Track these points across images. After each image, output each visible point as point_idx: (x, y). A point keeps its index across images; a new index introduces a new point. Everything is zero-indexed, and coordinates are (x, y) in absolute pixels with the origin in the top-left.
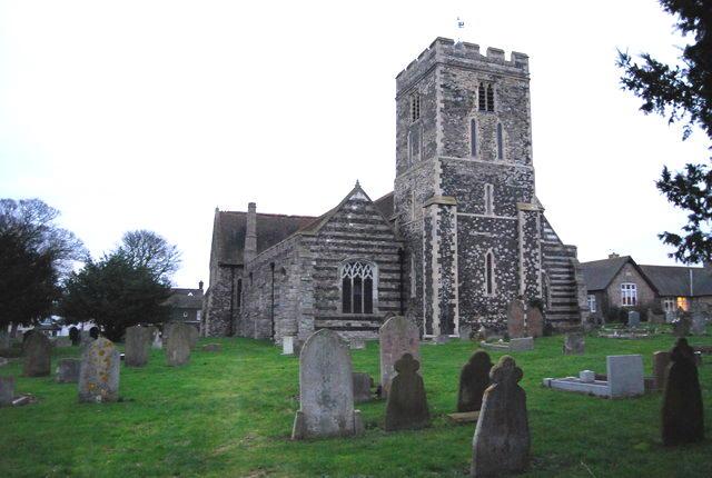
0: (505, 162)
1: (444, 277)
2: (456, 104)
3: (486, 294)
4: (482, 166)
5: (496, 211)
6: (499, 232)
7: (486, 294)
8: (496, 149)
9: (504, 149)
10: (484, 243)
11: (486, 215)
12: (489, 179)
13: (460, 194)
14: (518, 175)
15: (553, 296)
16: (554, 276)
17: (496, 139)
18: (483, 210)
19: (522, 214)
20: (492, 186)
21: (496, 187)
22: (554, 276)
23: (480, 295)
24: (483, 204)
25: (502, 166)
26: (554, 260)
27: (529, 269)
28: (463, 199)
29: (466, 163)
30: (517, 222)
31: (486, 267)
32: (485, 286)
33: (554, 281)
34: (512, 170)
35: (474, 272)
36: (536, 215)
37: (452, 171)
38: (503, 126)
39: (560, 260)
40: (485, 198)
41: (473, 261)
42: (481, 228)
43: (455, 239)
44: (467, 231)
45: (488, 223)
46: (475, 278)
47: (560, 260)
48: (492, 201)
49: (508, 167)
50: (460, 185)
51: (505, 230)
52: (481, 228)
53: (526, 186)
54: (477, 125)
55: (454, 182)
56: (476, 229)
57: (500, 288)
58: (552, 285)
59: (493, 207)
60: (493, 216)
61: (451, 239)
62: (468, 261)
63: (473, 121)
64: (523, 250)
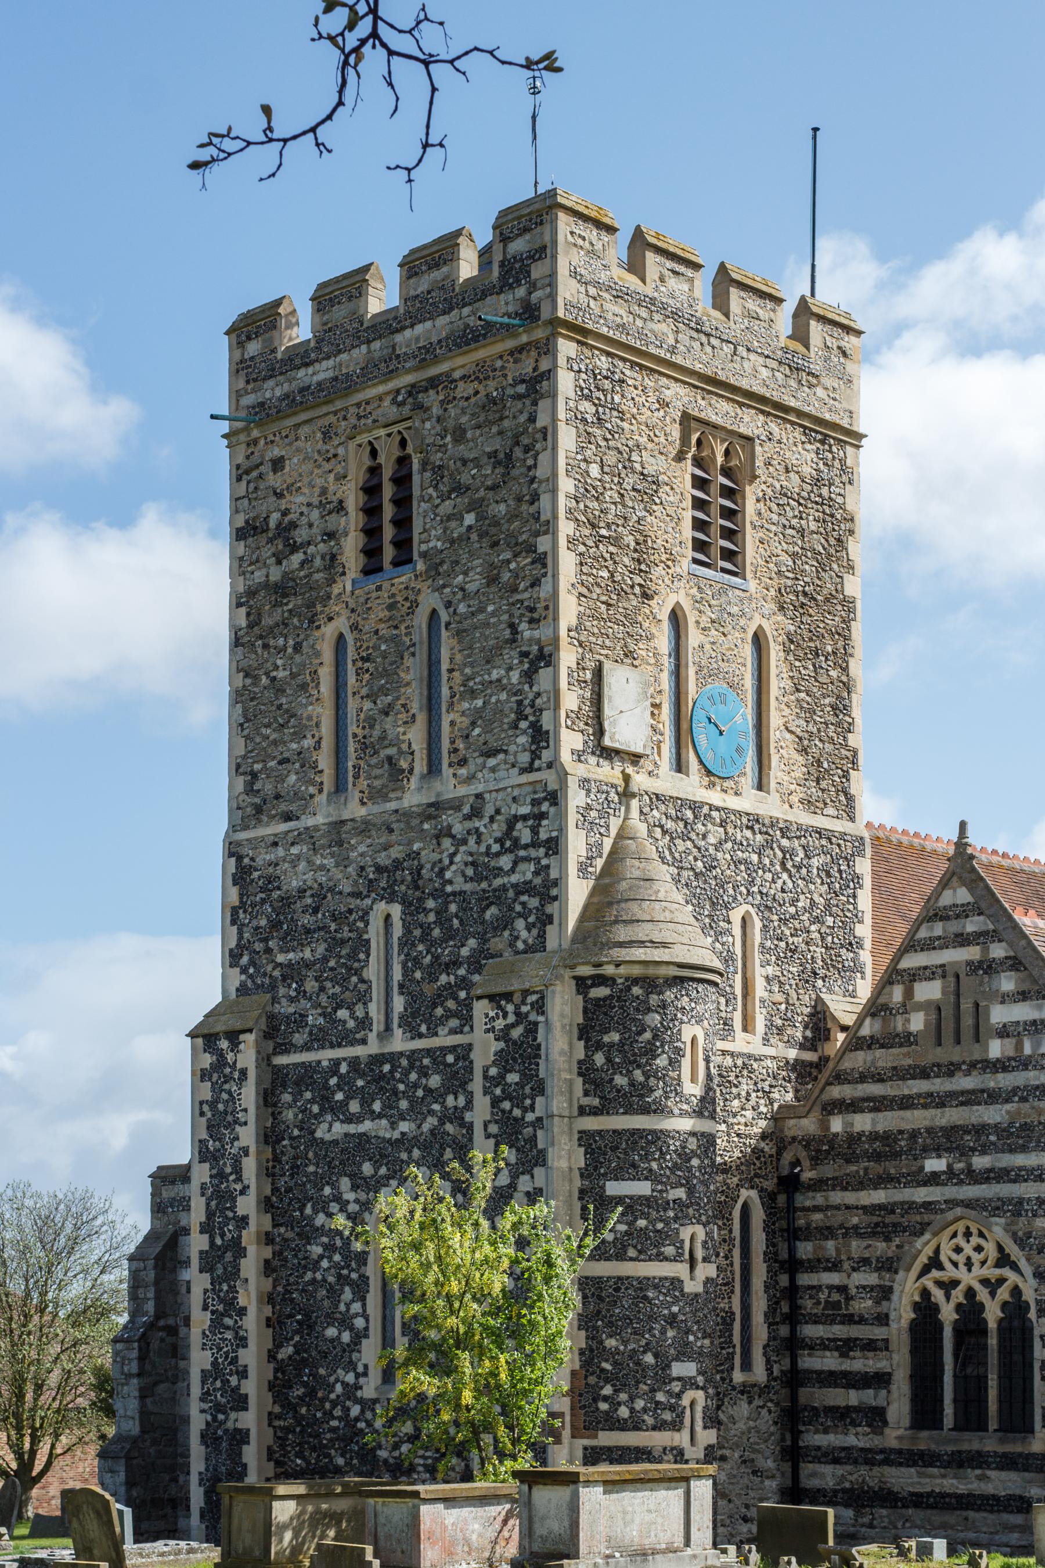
0: (450, 786)
1: (217, 1324)
2: (281, 590)
4: (364, 828)
5: (410, 1025)
6: (417, 1111)
7: (369, 1389)
8: (416, 736)
9: (446, 720)
10: (367, 1168)
11: (373, 1047)
12: (385, 880)
13: (292, 973)
14: (498, 828)
17: (414, 695)
18: (365, 1023)
19: (481, 1009)
20: (396, 910)
21: (412, 908)
23: (351, 1391)
24: (364, 998)
25: (436, 807)
28: (301, 992)
29: (307, 835)
30: (464, 1052)
34: (476, 813)
35: (334, 1294)
36: (540, 1007)
37: (271, 882)
38: (444, 616)
40: (373, 971)
41: (330, 1248)
42: (354, 1107)
43: (250, 1166)
44: (307, 1127)
45: (378, 1078)
46: (331, 1319)
48: (397, 974)
49: (455, 805)
50: (295, 937)
51: (437, 1094)
52: (354, 1107)
53: (526, 872)
54: (351, 653)
55: (275, 925)
56: (339, 1111)
59: (399, 1003)
60: (399, 1043)
61: (238, 1170)
62: (316, 1250)
63: (340, 640)
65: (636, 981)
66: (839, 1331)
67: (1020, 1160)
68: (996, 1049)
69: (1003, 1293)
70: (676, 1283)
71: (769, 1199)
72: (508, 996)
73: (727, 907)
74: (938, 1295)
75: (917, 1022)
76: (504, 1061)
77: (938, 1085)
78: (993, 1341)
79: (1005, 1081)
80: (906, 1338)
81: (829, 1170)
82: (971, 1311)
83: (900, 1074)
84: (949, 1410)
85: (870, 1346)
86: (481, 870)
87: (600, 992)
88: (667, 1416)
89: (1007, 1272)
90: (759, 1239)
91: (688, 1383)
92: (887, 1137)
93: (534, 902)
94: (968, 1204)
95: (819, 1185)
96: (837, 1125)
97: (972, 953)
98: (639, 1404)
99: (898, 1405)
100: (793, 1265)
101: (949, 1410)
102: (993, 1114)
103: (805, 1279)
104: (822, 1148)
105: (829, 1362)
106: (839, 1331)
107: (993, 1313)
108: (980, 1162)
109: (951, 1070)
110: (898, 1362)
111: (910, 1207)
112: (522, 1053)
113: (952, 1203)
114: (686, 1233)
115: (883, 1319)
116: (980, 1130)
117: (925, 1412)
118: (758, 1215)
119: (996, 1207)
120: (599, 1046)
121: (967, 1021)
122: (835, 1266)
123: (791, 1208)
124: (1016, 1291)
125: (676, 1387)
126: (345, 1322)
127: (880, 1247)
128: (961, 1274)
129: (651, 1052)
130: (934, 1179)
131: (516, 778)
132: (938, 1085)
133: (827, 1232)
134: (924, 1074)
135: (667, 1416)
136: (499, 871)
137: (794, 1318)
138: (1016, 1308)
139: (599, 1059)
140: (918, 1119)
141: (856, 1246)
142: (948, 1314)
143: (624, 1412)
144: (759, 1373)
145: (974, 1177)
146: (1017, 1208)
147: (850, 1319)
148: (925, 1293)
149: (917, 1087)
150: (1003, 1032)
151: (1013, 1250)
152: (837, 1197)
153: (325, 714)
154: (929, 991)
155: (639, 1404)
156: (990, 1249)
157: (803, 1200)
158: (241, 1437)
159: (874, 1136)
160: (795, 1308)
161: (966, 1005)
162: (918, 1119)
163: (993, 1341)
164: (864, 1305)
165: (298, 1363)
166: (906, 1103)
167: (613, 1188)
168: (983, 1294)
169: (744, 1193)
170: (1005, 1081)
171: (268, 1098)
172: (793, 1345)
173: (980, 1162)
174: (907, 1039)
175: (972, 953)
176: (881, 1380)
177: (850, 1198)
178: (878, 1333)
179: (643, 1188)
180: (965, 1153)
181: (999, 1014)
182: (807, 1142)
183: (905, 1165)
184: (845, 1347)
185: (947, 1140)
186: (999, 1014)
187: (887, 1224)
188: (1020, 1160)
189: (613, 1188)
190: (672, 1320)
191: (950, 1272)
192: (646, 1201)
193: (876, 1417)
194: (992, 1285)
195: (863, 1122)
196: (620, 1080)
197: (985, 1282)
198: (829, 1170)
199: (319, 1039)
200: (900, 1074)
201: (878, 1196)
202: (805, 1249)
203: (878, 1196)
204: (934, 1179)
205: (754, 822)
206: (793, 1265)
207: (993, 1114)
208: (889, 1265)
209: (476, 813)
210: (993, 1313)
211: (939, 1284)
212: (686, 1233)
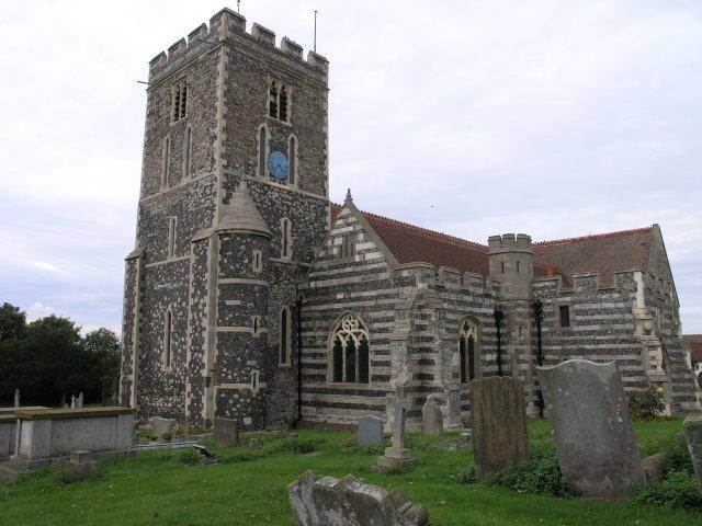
3: (163, 366)
6: (178, 280)
11: (169, 260)
15: (376, 364)
16: (376, 326)
18: (167, 253)
20: (176, 218)
21: (180, 216)
22: (376, 326)
23: (159, 368)
26: (377, 297)
27: (195, 329)
31: (165, 330)
32: (163, 358)
33: (377, 336)
34: (197, 187)
35: (156, 338)
39: (387, 296)
42: (163, 279)
47: (387, 296)
52: (163, 279)
57: (175, 359)
58: (373, 342)
64: (191, 301)
65: (238, 235)
66: (312, 351)
67: (365, 294)
68: (357, 258)
69: (360, 338)
70: (249, 334)
71: (292, 309)
72: (200, 241)
73: (279, 218)
74: (341, 338)
75: (335, 251)
76: (198, 262)
77: (341, 271)
78: (357, 353)
79: (359, 269)
80: (332, 353)
81: (311, 299)
82: (351, 343)
83: (330, 268)
84: (344, 376)
85: (321, 355)
86: (197, 204)
87: (226, 239)
88: (245, 379)
89: (361, 330)
90: (289, 320)
91: (252, 367)
92: (326, 288)
93: (209, 212)
94: (350, 309)
95: (307, 304)
96: (312, 284)
97: (351, 229)
98: (235, 374)
99: (330, 373)
100: (300, 330)
101: (344, 376)
102: (356, 279)
103: (303, 334)
104: (309, 293)
105: (310, 360)
106: (312, 351)
107: (357, 344)
108: (353, 295)
109: (345, 266)
110: (330, 361)
111: (332, 310)
112: (202, 260)
113: (345, 308)
114: (253, 318)
115: (325, 346)
116: (353, 284)
117: (338, 378)
118: (289, 314)
119: (357, 309)
120: (226, 256)
121: (349, 250)
122: (311, 330)
123: (299, 312)
124: (364, 336)
125: (248, 369)
126: (158, 347)
127: (325, 324)
128: (347, 331)
129: (242, 258)
130: (339, 301)
131: (207, 174)
132: (341, 271)
133: (310, 319)
134: (337, 268)
135: (245, 379)
136: (201, 203)
137: (300, 347)
138: (364, 342)
139: (225, 261)
140: (334, 282)
141: (318, 323)
142: (344, 344)
143: (230, 377)
144: (288, 364)
145: (352, 300)
146: (363, 309)
147: (315, 347)
148: (338, 338)
149: (335, 271)
150: (359, 253)
151: (363, 323)
152: (313, 308)
153: (163, 162)
154: (339, 241)
155: (235, 374)
156: (357, 324)
157: (304, 309)
158: (130, 382)
159: (323, 288)
160: (300, 343)
161: (349, 244)
162: (334, 282)
163: (357, 353)
164: (319, 342)
165: (147, 360)
166: (332, 277)
167: (228, 303)
168: (354, 337)
169: (284, 307)
170: (359, 269)
171: (142, 278)
172: (300, 355)
173: (353, 295)
174: (333, 257)
175: (351, 229)
176: (324, 366)
177: (316, 308)
178: (324, 351)
179: (238, 302)
180: (349, 292)
181: (359, 247)
182: (304, 291)
183: (330, 297)
184: (314, 356)
185: (345, 288)
186: (359, 247)
187: (326, 316)
188: (365, 294)
189: (228, 303)
190: (247, 346)
191: (345, 331)
192: (239, 307)
193: (323, 378)
194: (357, 334)
195: (320, 284)
196: (232, 267)
197: (355, 334)
198: (311, 299)
199: (157, 259)
200: (330, 268)
201: (324, 307)
202: (303, 325)
203: (324, 307)
204: (339, 301)
205: (289, 192)
206: (300, 330)
207: (356, 279)
208: (326, 329)
209: (197, 187)
210: (357, 344)
211: (342, 335)
212: (253, 318)
